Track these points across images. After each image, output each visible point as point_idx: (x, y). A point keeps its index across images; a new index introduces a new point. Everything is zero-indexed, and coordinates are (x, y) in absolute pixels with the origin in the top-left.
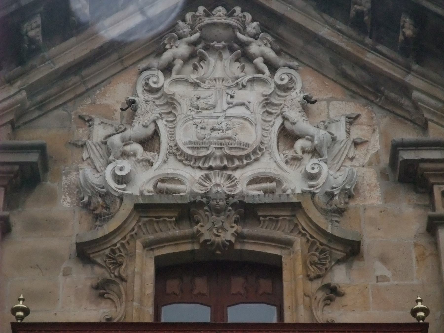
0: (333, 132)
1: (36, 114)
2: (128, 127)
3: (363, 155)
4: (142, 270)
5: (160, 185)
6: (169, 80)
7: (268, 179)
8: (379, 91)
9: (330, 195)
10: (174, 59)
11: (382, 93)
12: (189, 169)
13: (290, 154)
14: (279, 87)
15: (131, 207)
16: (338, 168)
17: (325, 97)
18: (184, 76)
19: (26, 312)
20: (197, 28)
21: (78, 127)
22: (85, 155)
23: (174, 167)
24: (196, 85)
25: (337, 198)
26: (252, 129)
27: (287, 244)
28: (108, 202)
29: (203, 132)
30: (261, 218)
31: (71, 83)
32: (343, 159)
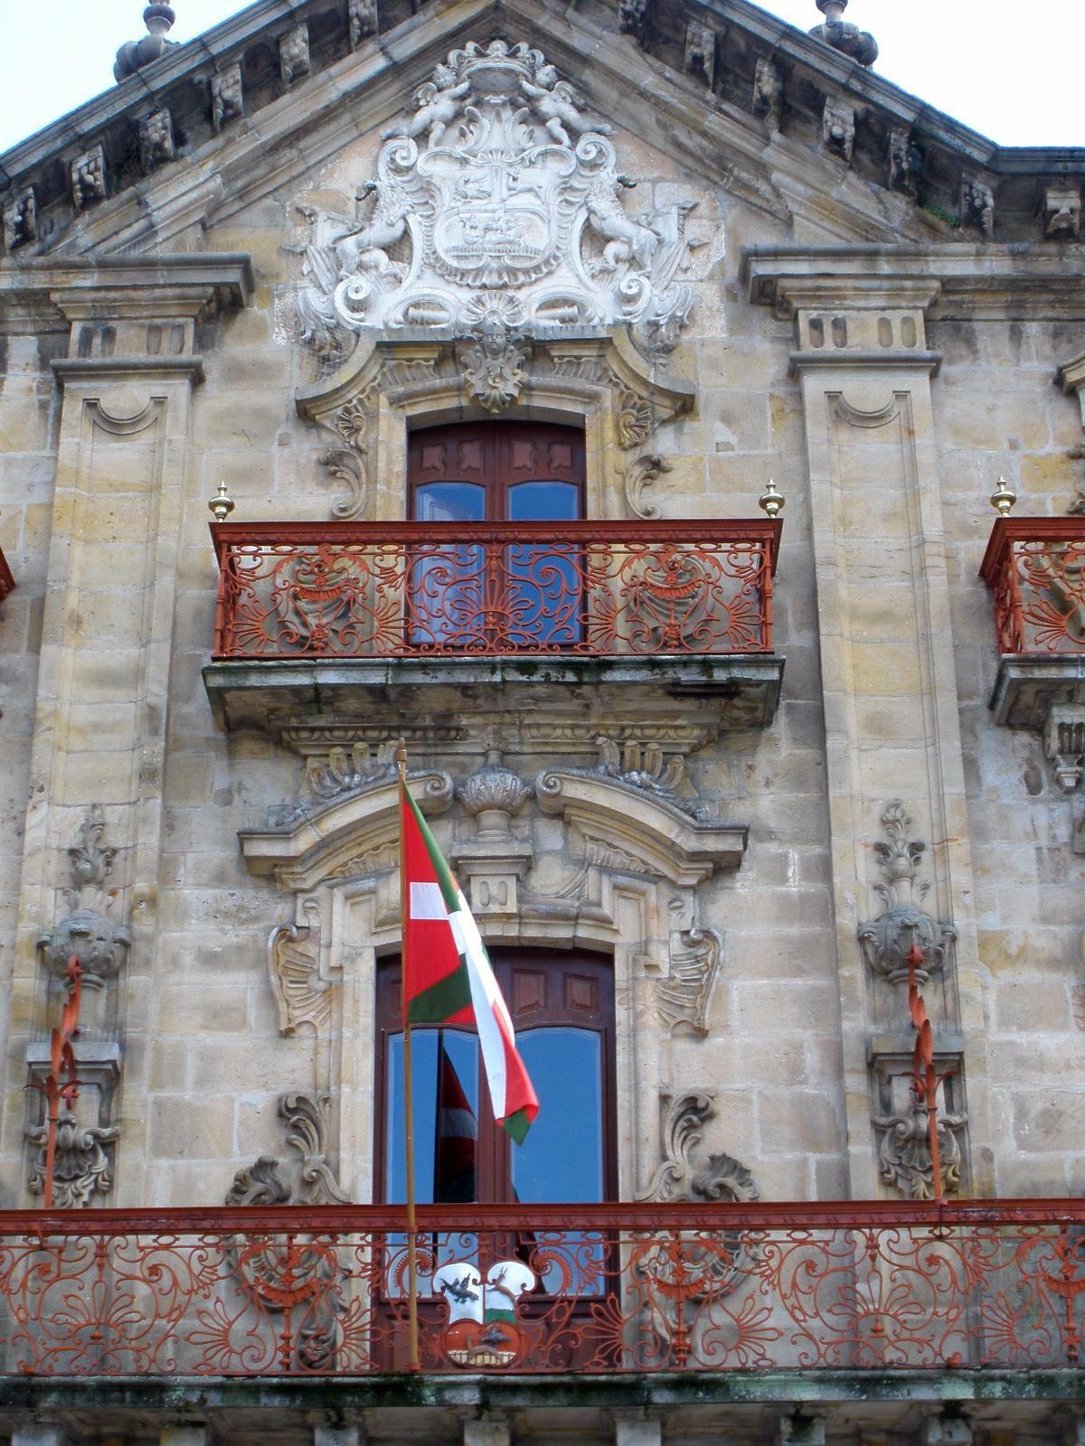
0: (660, 230)
1: (236, 207)
2: (366, 224)
3: (702, 265)
4: (390, 439)
5: (412, 312)
6: (424, 155)
7: (567, 302)
8: (725, 169)
9: (655, 326)
10: (432, 121)
11: (731, 171)
12: (453, 288)
13: (597, 264)
14: (582, 163)
15: (372, 346)
16: (666, 283)
17: (650, 176)
18: (447, 148)
19: (230, 506)
20: (464, 75)
21: (295, 225)
22: (305, 268)
23: (431, 286)
24: (463, 162)
25: (663, 330)
26: (543, 228)
27: (593, 398)
28: (339, 336)
29: (474, 233)
30: (556, 360)
31: (283, 161)
32: (673, 269)
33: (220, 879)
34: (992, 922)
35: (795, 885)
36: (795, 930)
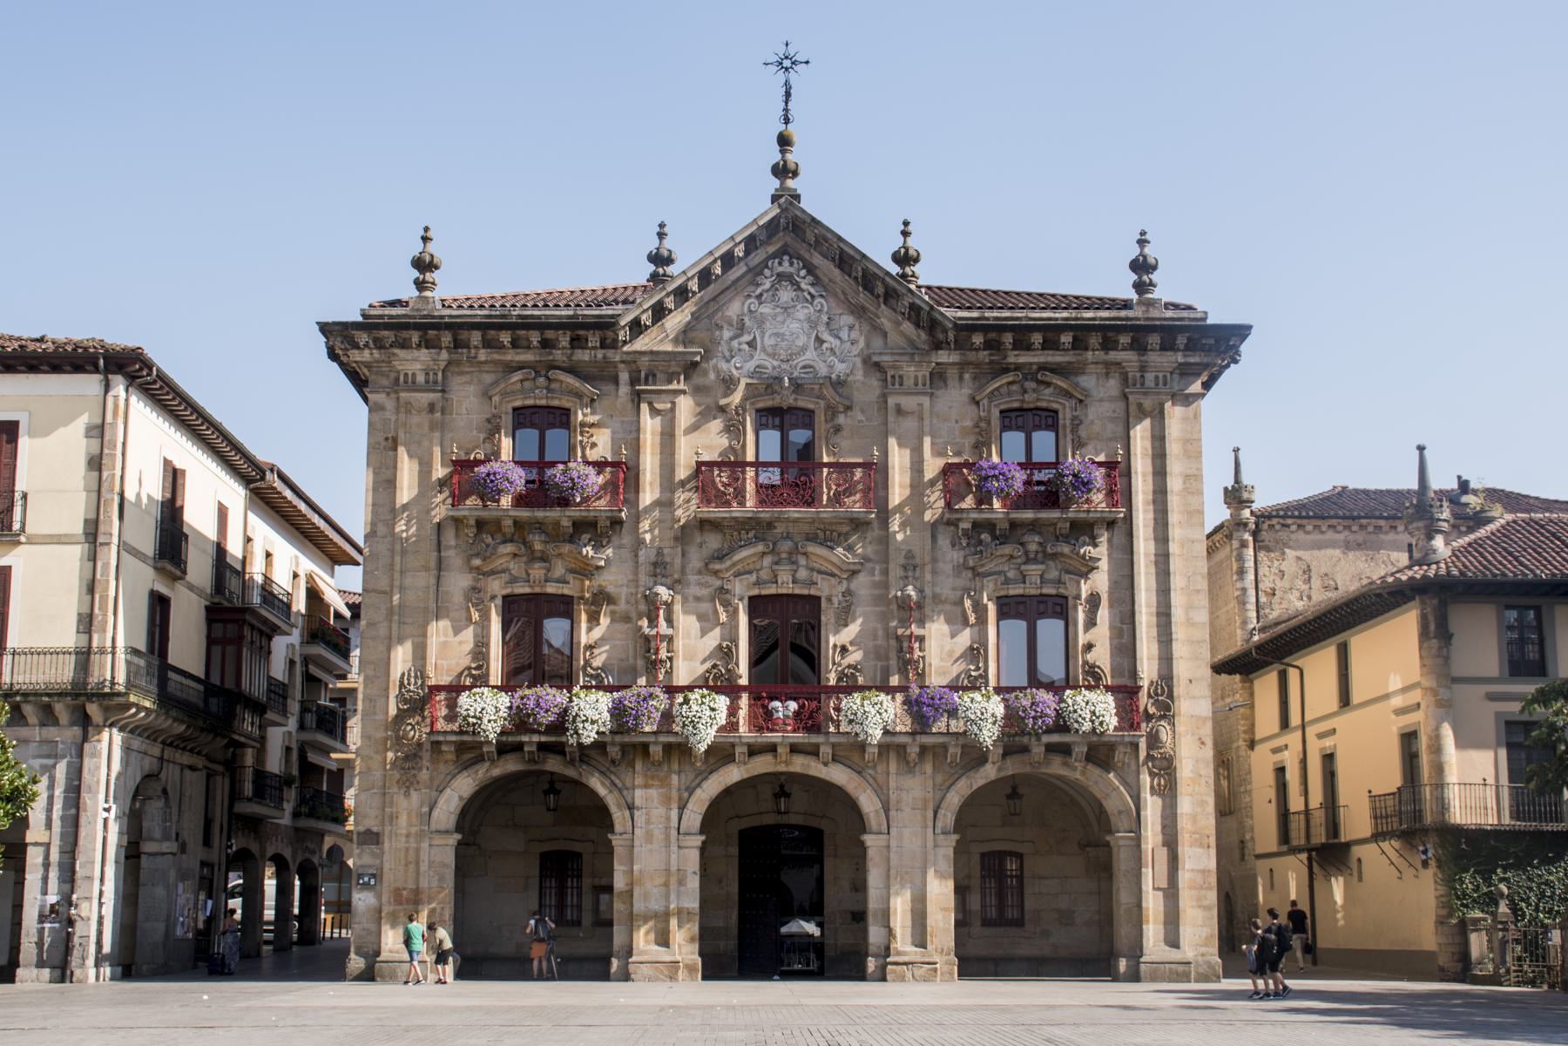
3: (856, 350)
33: (699, 572)
34: (938, 590)
35: (877, 578)
36: (876, 592)
